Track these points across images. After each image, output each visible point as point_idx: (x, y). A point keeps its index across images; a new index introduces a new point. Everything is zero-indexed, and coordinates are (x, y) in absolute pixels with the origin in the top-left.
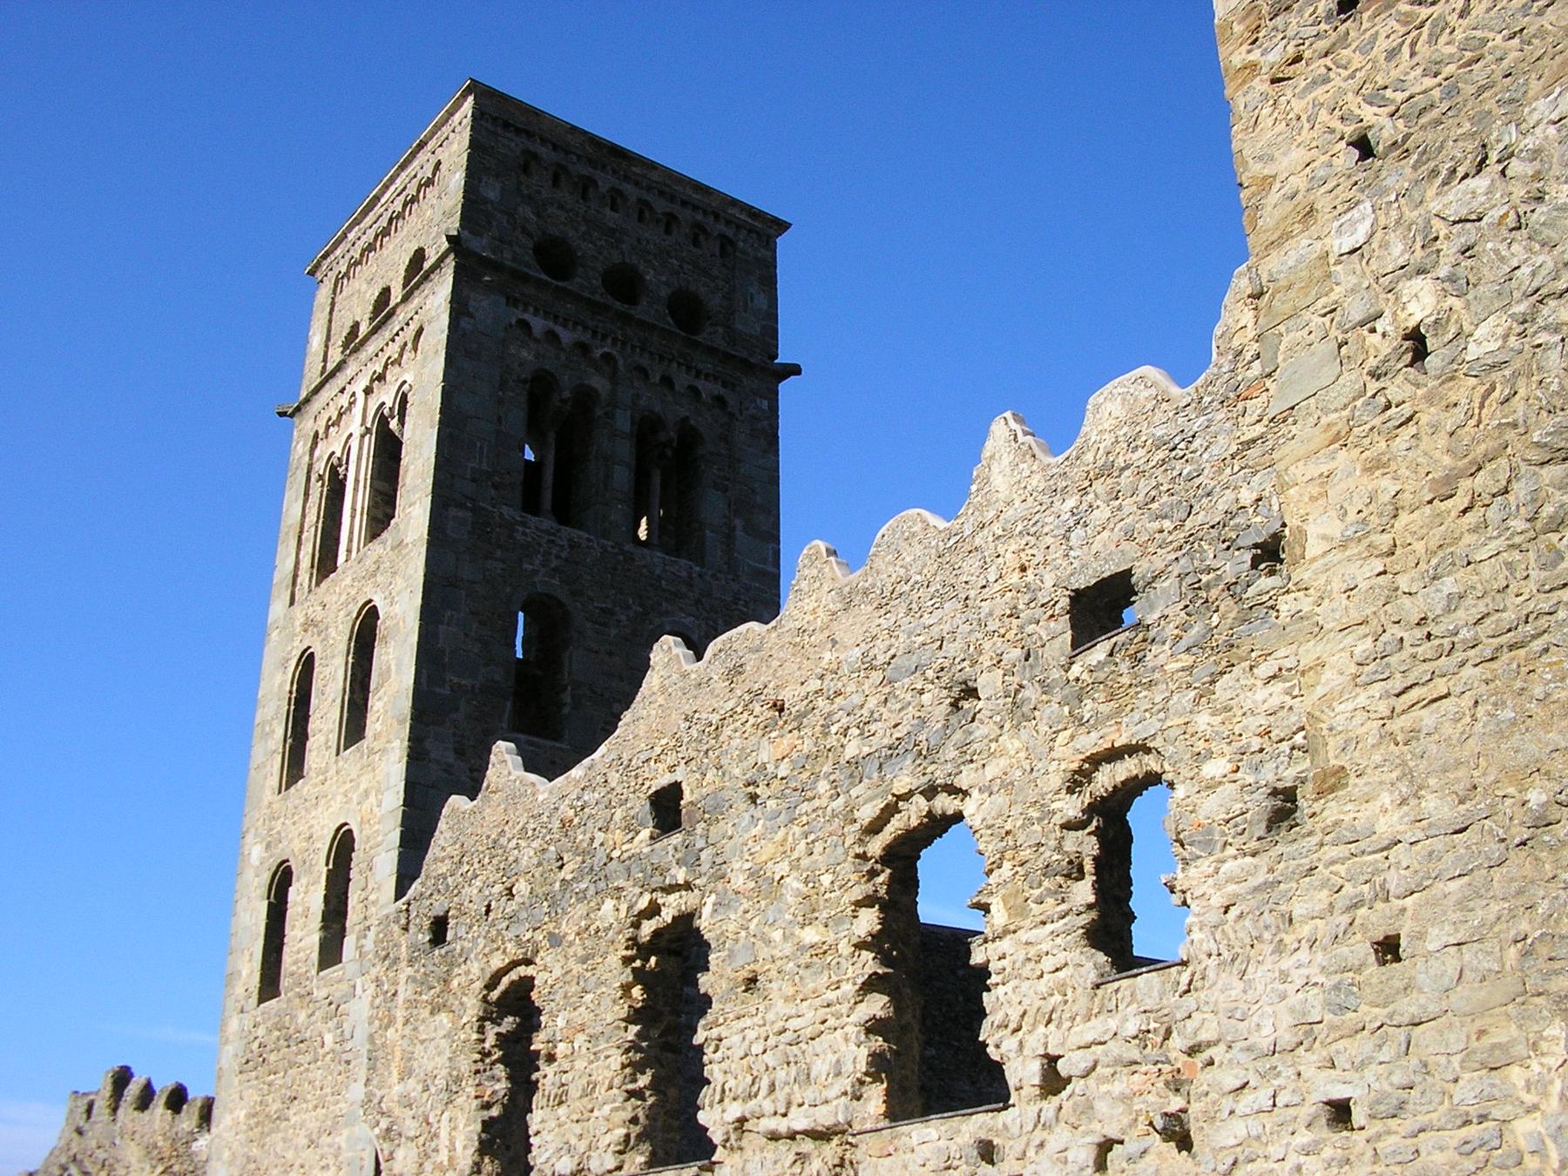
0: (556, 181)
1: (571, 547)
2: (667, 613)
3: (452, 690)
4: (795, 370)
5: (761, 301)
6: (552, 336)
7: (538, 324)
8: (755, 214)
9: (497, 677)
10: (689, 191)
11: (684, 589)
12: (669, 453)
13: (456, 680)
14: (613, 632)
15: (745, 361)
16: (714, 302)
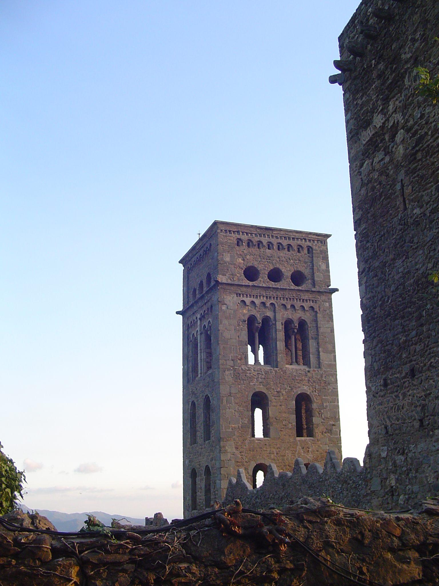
0: (248, 246)
1: (266, 374)
2: (299, 387)
3: (232, 429)
4: (336, 290)
5: (323, 267)
6: (253, 302)
7: (248, 300)
8: (318, 235)
9: (246, 422)
10: (294, 234)
11: (303, 377)
12: (296, 331)
13: (233, 426)
14: (282, 398)
15: (319, 292)
16: (306, 272)
